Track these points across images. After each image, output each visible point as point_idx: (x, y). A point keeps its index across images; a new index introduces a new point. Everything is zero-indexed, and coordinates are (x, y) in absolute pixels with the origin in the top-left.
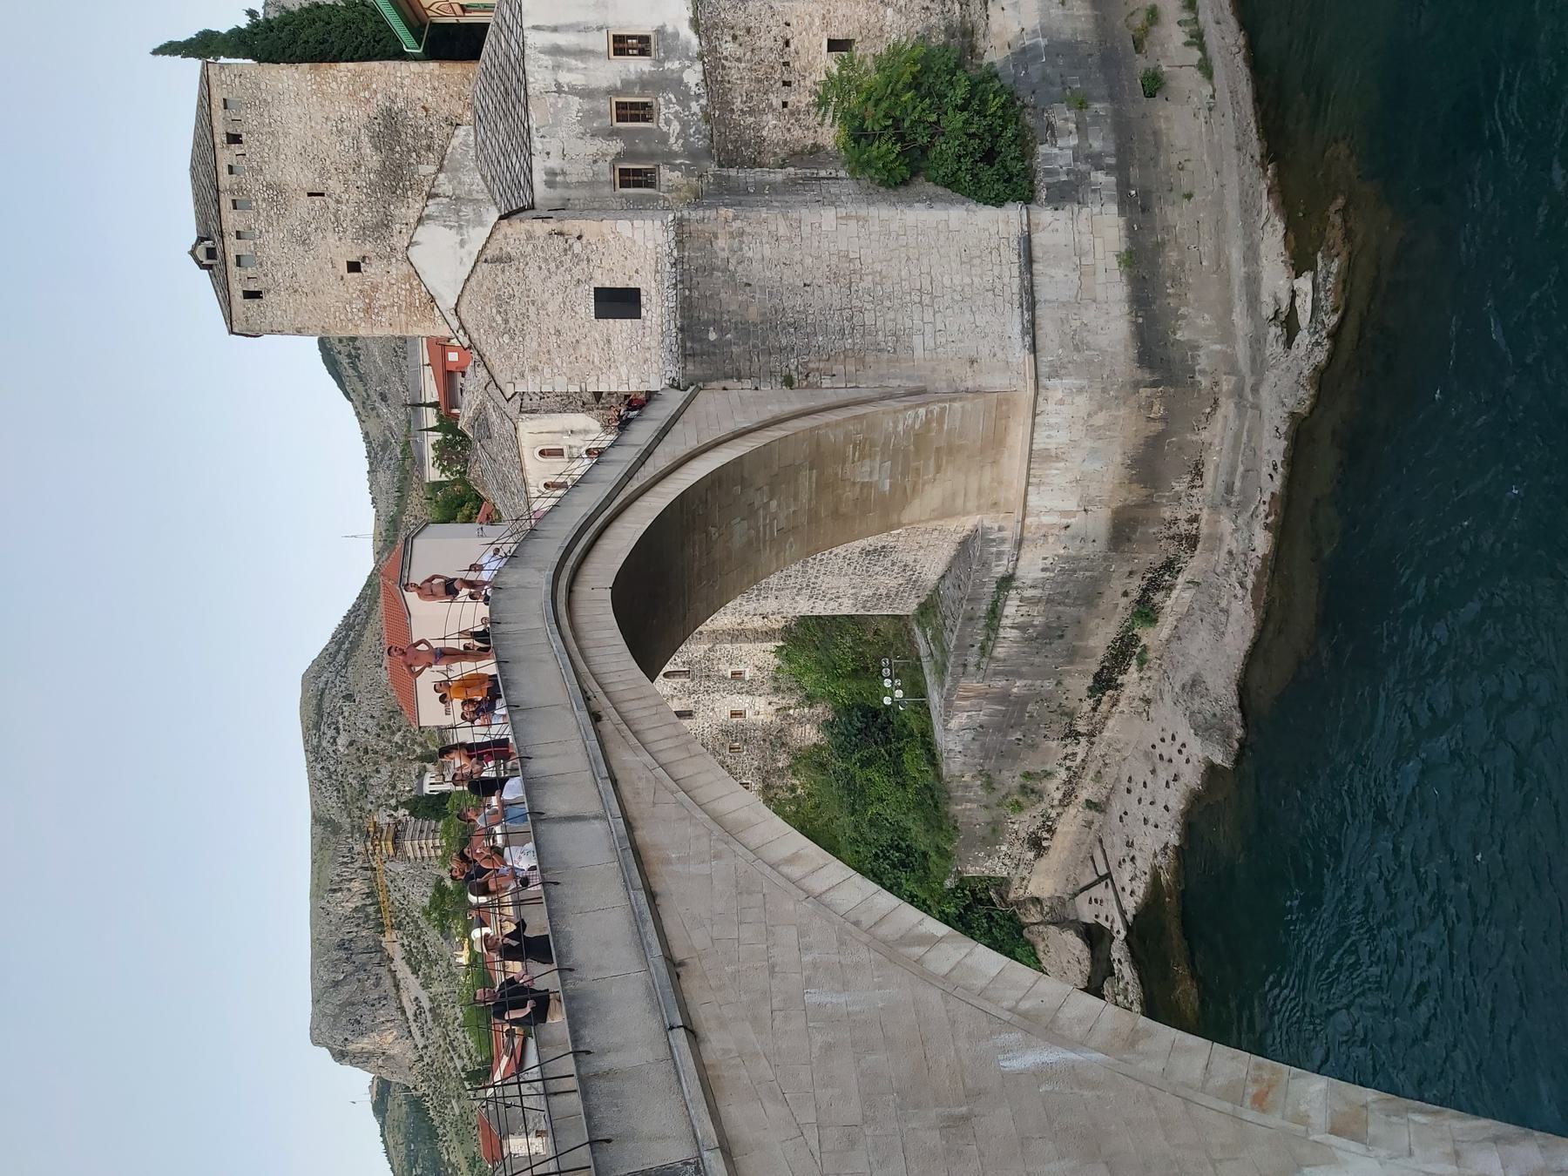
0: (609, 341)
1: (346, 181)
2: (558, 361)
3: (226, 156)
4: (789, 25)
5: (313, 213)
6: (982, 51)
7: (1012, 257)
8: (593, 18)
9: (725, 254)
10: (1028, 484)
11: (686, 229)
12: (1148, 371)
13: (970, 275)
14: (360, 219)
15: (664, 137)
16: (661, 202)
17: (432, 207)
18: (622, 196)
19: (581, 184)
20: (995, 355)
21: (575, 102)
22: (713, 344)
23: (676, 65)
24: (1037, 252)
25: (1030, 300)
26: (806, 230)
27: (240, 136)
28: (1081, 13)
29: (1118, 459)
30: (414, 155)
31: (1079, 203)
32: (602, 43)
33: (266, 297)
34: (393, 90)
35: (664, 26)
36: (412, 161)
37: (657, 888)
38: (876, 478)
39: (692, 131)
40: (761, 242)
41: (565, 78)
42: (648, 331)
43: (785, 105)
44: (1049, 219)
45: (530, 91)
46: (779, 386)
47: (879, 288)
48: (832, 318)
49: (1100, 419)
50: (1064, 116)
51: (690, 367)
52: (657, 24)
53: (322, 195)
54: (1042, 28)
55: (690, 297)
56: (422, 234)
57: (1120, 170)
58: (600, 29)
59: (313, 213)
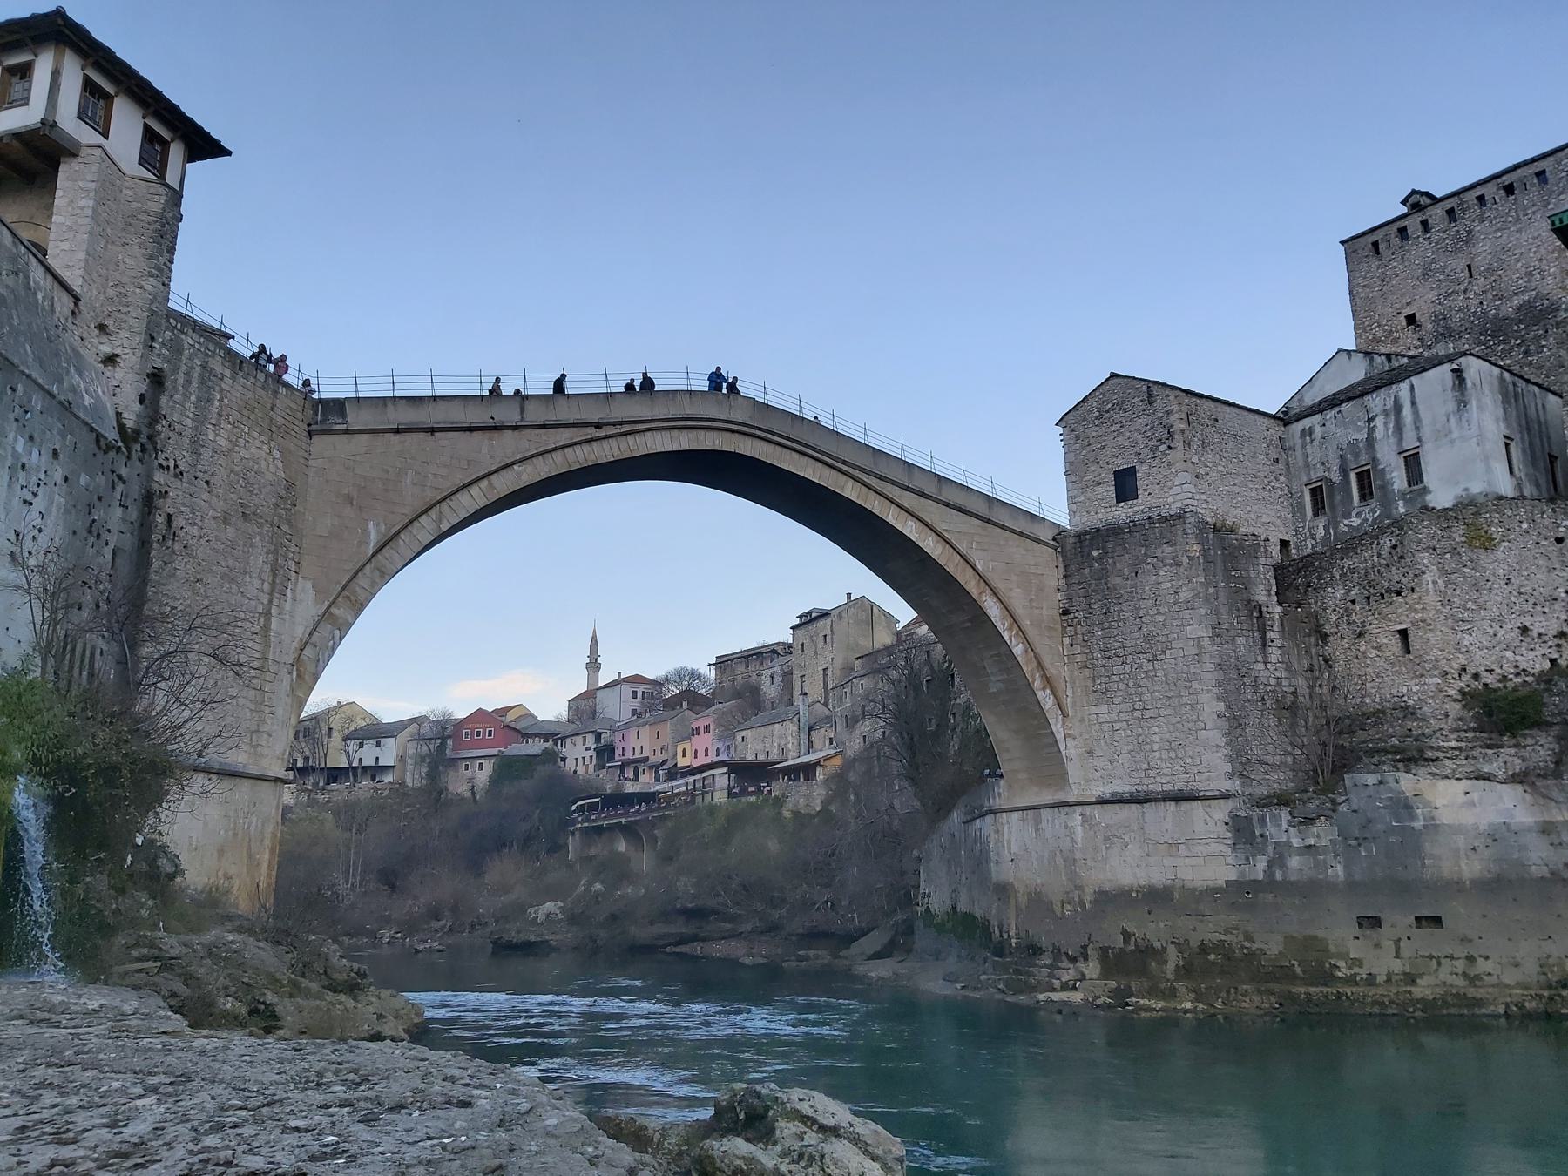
0: (1100, 484)
4: (1413, 590)
6: (1413, 771)
7: (1179, 784)
8: (1426, 431)
11: (1177, 522)
13: (1160, 749)
15: (1347, 515)
16: (1302, 524)
18: (1302, 492)
22: (1089, 554)
24: (1185, 806)
25: (1141, 799)
27: (1513, 194)
29: (1039, 881)
30: (1519, 341)
32: (1410, 442)
33: (1375, 263)
35: (1430, 492)
36: (1513, 341)
37: (475, 434)
38: (992, 678)
41: (1379, 421)
42: (1109, 510)
43: (1353, 602)
44: (1216, 817)
45: (1366, 398)
48: (1116, 641)
49: (1059, 861)
50: (1322, 835)
51: (1071, 540)
52: (1431, 487)
53: (1471, 276)
54: (1436, 826)
55: (1124, 533)
57: (1269, 884)
58: (1419, 439)
59: (1452, 274)
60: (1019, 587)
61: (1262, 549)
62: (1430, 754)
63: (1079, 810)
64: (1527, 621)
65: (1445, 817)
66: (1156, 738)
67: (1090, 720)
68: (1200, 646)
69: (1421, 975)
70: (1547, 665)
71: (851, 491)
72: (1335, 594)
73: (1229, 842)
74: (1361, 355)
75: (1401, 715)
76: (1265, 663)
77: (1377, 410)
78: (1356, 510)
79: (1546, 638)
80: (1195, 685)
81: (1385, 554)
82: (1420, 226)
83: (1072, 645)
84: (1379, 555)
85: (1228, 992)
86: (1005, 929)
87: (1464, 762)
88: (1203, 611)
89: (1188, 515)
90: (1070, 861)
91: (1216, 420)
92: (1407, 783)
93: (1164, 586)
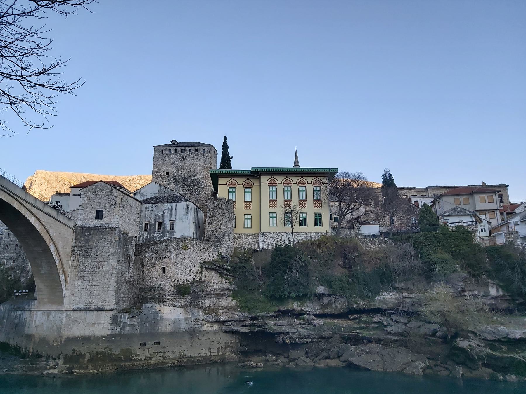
0: (91, 212)
1: (186, 173)
2: (87, 201)
3: (192, 148)
5: (180, 166)
6: (160, 304)
8: (177, 217)
9: (106, 238)
10: (43, 311)
11: (113, 230)
12: (65, 340)
14: (178, 176)
15: (154, 233)
17: (163, 187)
19: (146, 214)
20: (74, 300)
21: (162, 213)
22: (85, 234)
23: (168, 235)
24: (100, 312)
26: (111, 257)
27: (197, 152)
28: (167, 329)
29: (45, 334)
30: (191, 188)
31: (112, 323)
33: (161, 156)
34: (206, 185)
36: (190, 188)
38: (44, 269)
39: (155, 239)
40: (109, 246)
41: (167, 211)
42: (92, 221)
43: (153, 258)
44: (108, 316)
46: (72, 248)
47: (94, 273)
49: (55, 328)
51: (80, 228)
53: (184, 168)
55: (97, 230)
56: (157, 185)
57: (120, 335)
58: (175, 219)
59: (180, 166)
60: (61, 242)
61: (133, 240)
62: (165, 300)
63: (65, 312)
64: (191, 268)
65: (165, 316)
66: (95, 292)
67: (75, 285)
68: (113, 267)
69: (152, 358)
70: (193, 280)
71: (16, 205)
72: (148, 255)
73: (110, 323)
74: (158, 185)
75: (159, 289)
76: (128, 272)
77: (167, 208)
78: (156, 232)
79: (194, 273)
80: (110, 277)
81: (163, 247)
82: (174, 151)
83: (73, 261)
84: (162, 247)
85: (103, 366)
86: (28, 349)
87: (172, 302)
88: (116, 256)
89: (117, 228)
90: (59, 328)
91: (127, 201)
92: (158, 307)
93: (106, 247)
